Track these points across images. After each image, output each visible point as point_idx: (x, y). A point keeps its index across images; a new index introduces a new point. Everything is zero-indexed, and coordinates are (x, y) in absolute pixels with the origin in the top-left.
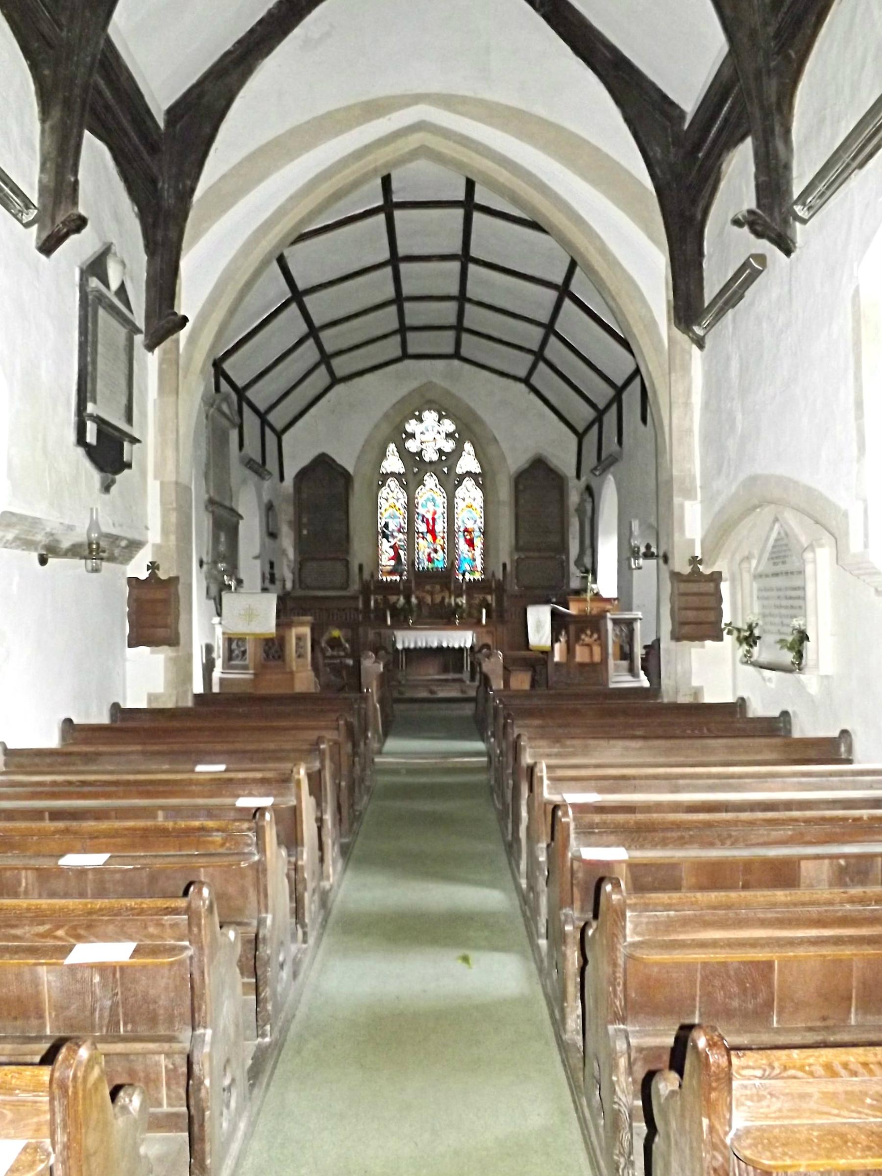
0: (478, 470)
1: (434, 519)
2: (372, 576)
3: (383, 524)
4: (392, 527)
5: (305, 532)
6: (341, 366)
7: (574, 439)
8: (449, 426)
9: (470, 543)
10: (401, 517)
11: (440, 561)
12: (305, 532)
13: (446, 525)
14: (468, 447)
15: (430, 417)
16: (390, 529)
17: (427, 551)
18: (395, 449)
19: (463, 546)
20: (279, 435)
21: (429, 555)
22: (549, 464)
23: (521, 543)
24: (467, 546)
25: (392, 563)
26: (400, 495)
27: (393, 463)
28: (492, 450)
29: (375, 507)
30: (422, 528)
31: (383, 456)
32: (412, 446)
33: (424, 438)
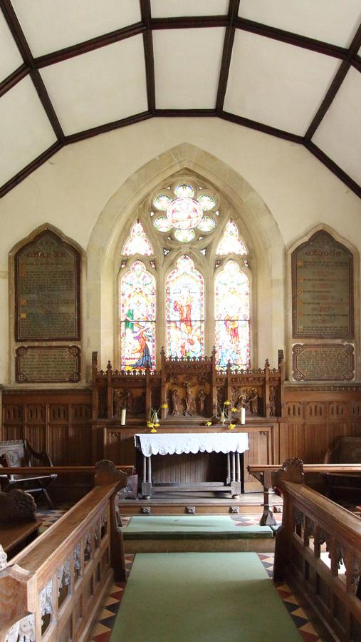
1: (189, 307)
2: (109, 366)
5: (24, 316)
8: (207, 203)
9: (235, 333)
11: (197, 352)
12: (24, 316)
13: (203, 313)
14: (231, 228)
15: (184, 193)
16: (135, 318)
21: (183, 347)
22: (334, 236)
24: (230, 337)
25: (138, 355)
27: (138, 244)
29: (116, 294)
30: (175, 316)
31: (126, 233)
32: (162, 225)
33: (176, 216)
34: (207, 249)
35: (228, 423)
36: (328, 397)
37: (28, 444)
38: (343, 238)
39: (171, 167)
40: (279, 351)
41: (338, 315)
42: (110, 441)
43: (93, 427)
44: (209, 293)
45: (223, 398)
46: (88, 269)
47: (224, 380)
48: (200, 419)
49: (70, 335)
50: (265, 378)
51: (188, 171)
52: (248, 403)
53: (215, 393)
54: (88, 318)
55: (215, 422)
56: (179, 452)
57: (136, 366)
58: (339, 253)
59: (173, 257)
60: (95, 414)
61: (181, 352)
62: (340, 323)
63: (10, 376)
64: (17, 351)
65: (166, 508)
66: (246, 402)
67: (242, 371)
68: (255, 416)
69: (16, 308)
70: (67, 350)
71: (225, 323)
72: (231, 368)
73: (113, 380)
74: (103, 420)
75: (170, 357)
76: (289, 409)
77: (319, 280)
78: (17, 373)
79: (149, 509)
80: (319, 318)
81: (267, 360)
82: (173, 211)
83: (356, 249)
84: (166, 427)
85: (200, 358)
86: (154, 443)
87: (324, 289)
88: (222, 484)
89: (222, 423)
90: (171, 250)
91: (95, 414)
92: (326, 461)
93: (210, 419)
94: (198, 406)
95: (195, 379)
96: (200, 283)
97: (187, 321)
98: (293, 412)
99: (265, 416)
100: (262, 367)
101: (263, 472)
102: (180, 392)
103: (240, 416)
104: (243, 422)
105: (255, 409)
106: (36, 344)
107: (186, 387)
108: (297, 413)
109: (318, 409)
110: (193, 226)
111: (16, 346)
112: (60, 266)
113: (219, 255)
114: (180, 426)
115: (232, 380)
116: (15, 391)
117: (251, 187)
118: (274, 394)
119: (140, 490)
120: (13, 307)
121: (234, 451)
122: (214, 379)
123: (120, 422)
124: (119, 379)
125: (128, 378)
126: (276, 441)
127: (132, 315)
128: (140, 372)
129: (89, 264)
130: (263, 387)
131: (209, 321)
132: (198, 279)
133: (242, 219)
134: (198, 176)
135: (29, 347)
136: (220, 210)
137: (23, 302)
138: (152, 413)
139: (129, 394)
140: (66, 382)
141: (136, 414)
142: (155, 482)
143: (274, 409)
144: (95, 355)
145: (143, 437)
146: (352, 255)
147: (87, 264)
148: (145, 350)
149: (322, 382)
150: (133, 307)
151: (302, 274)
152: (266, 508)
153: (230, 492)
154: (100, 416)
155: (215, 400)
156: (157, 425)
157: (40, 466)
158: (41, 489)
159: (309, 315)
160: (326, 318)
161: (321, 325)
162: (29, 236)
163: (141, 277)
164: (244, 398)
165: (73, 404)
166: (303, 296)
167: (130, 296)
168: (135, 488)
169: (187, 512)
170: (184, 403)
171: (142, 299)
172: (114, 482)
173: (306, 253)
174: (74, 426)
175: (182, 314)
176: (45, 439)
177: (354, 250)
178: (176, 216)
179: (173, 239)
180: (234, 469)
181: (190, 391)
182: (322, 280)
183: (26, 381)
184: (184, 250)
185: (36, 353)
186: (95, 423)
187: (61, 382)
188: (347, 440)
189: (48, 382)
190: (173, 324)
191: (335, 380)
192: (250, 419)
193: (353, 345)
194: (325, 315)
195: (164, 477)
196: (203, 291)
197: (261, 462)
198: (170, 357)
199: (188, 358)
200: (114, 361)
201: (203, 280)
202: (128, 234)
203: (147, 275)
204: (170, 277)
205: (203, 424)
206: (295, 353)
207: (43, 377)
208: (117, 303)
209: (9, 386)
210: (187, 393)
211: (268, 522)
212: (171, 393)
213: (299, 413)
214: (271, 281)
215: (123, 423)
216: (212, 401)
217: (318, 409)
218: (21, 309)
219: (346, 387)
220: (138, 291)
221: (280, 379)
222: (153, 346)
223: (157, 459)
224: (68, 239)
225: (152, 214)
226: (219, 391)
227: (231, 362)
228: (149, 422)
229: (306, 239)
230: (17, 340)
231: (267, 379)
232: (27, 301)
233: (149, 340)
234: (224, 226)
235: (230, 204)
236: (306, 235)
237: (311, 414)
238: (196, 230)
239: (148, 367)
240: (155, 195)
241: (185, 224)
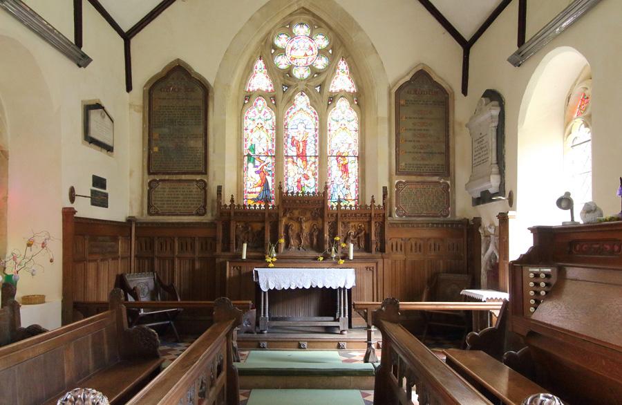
0: (353, 89)
1: (305, 142)
2: (232, 201)
3: (248, 147)
4: (259, 150)
5: (156, 149)
8: (322, 42)
9: (345, 169)
10: (269, 140)
11: (311, 187)
12: (156, 149)
13: (317, 148)
14: (343, 65)
15: (301, 31)
16: (257, 153)
17: (297, 177)
18: (263, 65)
21: (299, 181)
22: (433, 76)
24: (340, 173)
25: (259, 189)
27: (260, 81)
29: (240, 128)
30: (292, 151)
31: (249, 70)
32: (282, 62)
33: (294, 54)
34: (322, 86)
35: (337, 259)
36: (426, 233)
37: (157, 276)
38: (440, 78)
39: (289, 6)
40: (384, 187)
41: (436, 153)
42: (232, 275)
43: (217, 260)
44: (322, 129)
45: (334, 233)
46: (215, 104)
47: (335, 215)
48: (312, 254)
49: (197, 169)
50: (371, 214)
51: (305, 11)
52: (356, 239)
53: (327, 227)
54: (214, 152)
55: (326, 257)
56: (293, 288)
57: (255, 200)
59: (291, 94)
61: (298, 186)
62: (437, 161)
63: (143, 209)
64: (150, 184)
65: (281, 343)
66: (355, 238)
67: (351, 206)
68: (362, 251)
69: (149, 141)
70: (195, 183)
71: (337, 159)
72: (342, 204)
73: (235, 213)
75: (287, 193)
76: (392, 246)
77: (420, 118)
78: (149, 206)
79: (265, 344)
80: (420, 155)
81: (373, 196)
82: (292, 49)
83: (451, 88)
84: (283, 262)
85: (313, 193)
86: (272, 278)
87: (424, 128)
88: (332, 318)
89: (332, 258)
90: (289, 86)
92: (424, 296)
93: (322, 254)
96: (314, 119)
97: (302, 156)
98: (396, 248)
99: (371, 252)
100: (368, 203)
101: (367, 309)
102: (295, 226)
103: (349, 251)
104: (351, 258)
105: (362, 245)
106: (167, 177)
107: (300, 223)
108: (399, 249)
109: (418, 245)
110: (309, 64)
111: (148, 179)
112: (189, 101)
113: (331, 92)
114: (297, 261)
115: (342, 216)
116: (147, 223)
117: (359, 27)
118: (379, 230)
119: (257, 324)
120: (147, 141)
121: (342, 287)
122: (326, 215)
123: (241, 255)
124: (241, 213)
125: (249, 212)
126: (380, 277)
127: (254, 150)
128: (260, 206)
129: (215, 96)
130: (369, 223)
131: (322, 157)
132: (313, 115)
133: (352, 58)
134: (314, 15)
135: (160, 180)
136: (332, 49)
137: (156, 136)
138: (270, 247)
139: (250, 229)
140: (193, 215)
141: (256, 248)
142: (272, 316)
143: (379, 245)
144: (220, 189)
145: (262, 272)
146: (448, 94)
147: (213, 98)
149: (421, 219)
150: (255, 141)
152: (369, 345)
153: (338, 327)
154: (223, 250)
155: (326, 235)
156: (275, 259)
157: (169, 300)
158: (168, 322)
159: (410, 152)
160: (425, 155)
161: (422, 163)
162: (162, 71)
163: (263, 112)
164: (353, 234)
165: (199, 238)
167: (252, 131)
168: (254, 323)
169: (300, 347)
170: (299, 237)
171: (263, 135)
172: (230, 319)
173: (408, 92)
174: (201, 259)
175: (298, 149)
176: (173, 271)
177: (448, 88)
178: (294, 54)
179: (291, 76)
180: (343, 306)
182: (422, 118)
183: (157, 214)
184: (301, 87)
185: (168, 185)
186: (219, 257)
187: (190, 215)
188: (443, 276)
189: (177, 215)
190: (290, 159)
191: (433, 217)
192: (358, 254)
193: (449, 182)
194: (424, 153)
195: (280, 311)
196: (317, 127)
197: (366, 300)
198: (287, 193)
199: (303, 193)
200: (237, 194)
201: (317, 116)
202: (252, 70)
203: (267, 111)
204: (288, 113)
205: (316, 259)
206: (398, 190)
207: (173, 210)
208: (241, 138)
209: (142, 218)
210: (302, 228)
211: (370, 360)
212: (287, 228)
213: (401, 249)
214: (377, 118)
215: (244, 257)
216: (324, 235)
217: (418, 245)
218: (153, 143)
219: (442, 224)
220: (260, 126)
221: (384, 215)
222: (273, 181)
223: (273, 292)
224: (197, 74)
225: (273, 51)
226: (330, 226)
227: (342, 197)
228: (267, 256)
229: (408, 78)
230: (150, 173)
231: (373, 214)
232: (160, 135)
233: (269, 175)
234: (337, 65)
235: (342, 42)
236: (408, 74)
237: (411, 250)
238: (312, 67)
239: (267, 200)
240: (275, 33)
241: (302, 62)
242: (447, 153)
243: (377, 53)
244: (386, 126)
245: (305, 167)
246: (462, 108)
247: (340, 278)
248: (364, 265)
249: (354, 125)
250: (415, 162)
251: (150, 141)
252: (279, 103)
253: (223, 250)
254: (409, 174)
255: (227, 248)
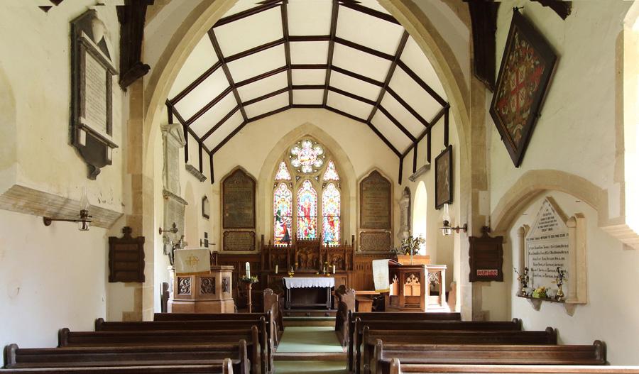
1: (309, 209)
2: (270, 243)
5: (227, 215)
6: (252, 111)
7: (398, 159)
8: (319, 151)
9: (332, 224)
11: (312, 236)
12: (227, 215)
14: (331, 165)
15: (307, 145)
17: (305, 228)
19: (327, 226)
20: (211, 154)
21: (306, 231)
23: (364, 223)
24: (329, 226)
25: (283, 235)
26: (288, 194)
27: (283, 174)
28: (346, 166)
29: (272, 201)
30: (302, 214)
31: (277, 169)
32: (296, 163)
33: (303, 158)
35: (326, 273)
44: (319, 202)
48: (314, 271)
49: (250, 226)
51: (308, 135)
53: (321, 257)
57: (281, 242)
58: (383, 183)
60: (263, 268)
62: (384, 220)
73: (272, 250)
74: (266, 271)
84: (297, 274)
90: (300, 177)
91: (263, 268)
94: (313, 263)
95: (311, 250)
105: (341, 267)
106: (233, 230)
107: (307, 255)
111: (223, 231)
130: (345, 254)
131: (319, 216)
137: (227, 207)
144: (263, 236)
148: (286, 233)
151: (365, 194)
154: (265, 269)
155: (321, 261)
166: (364, 205)
170: (306, 262)
171: (285, 205)
178: (303, 158)
181: (309, 256)
183: (228, 250)
185: (233, 234)
205: (315, 273)
212: (299, 257)
215: (277, 272)
223: (293, 290)
229: (367, 175)
230: (224, 228)
238: (313, 166)
241: (308, 163)
242: (390, 216)
243: (349, 161)
244: (355, 202)
245: (309, 223)
246: (398, 192)
247: (328, 282)
248: (341, 277)
249: (338, 199)
250: (373, 221)
251: (224, 211)
252: (294, 187)
253: (265, 269)
254: (367, 228)
255: (267, 267)
